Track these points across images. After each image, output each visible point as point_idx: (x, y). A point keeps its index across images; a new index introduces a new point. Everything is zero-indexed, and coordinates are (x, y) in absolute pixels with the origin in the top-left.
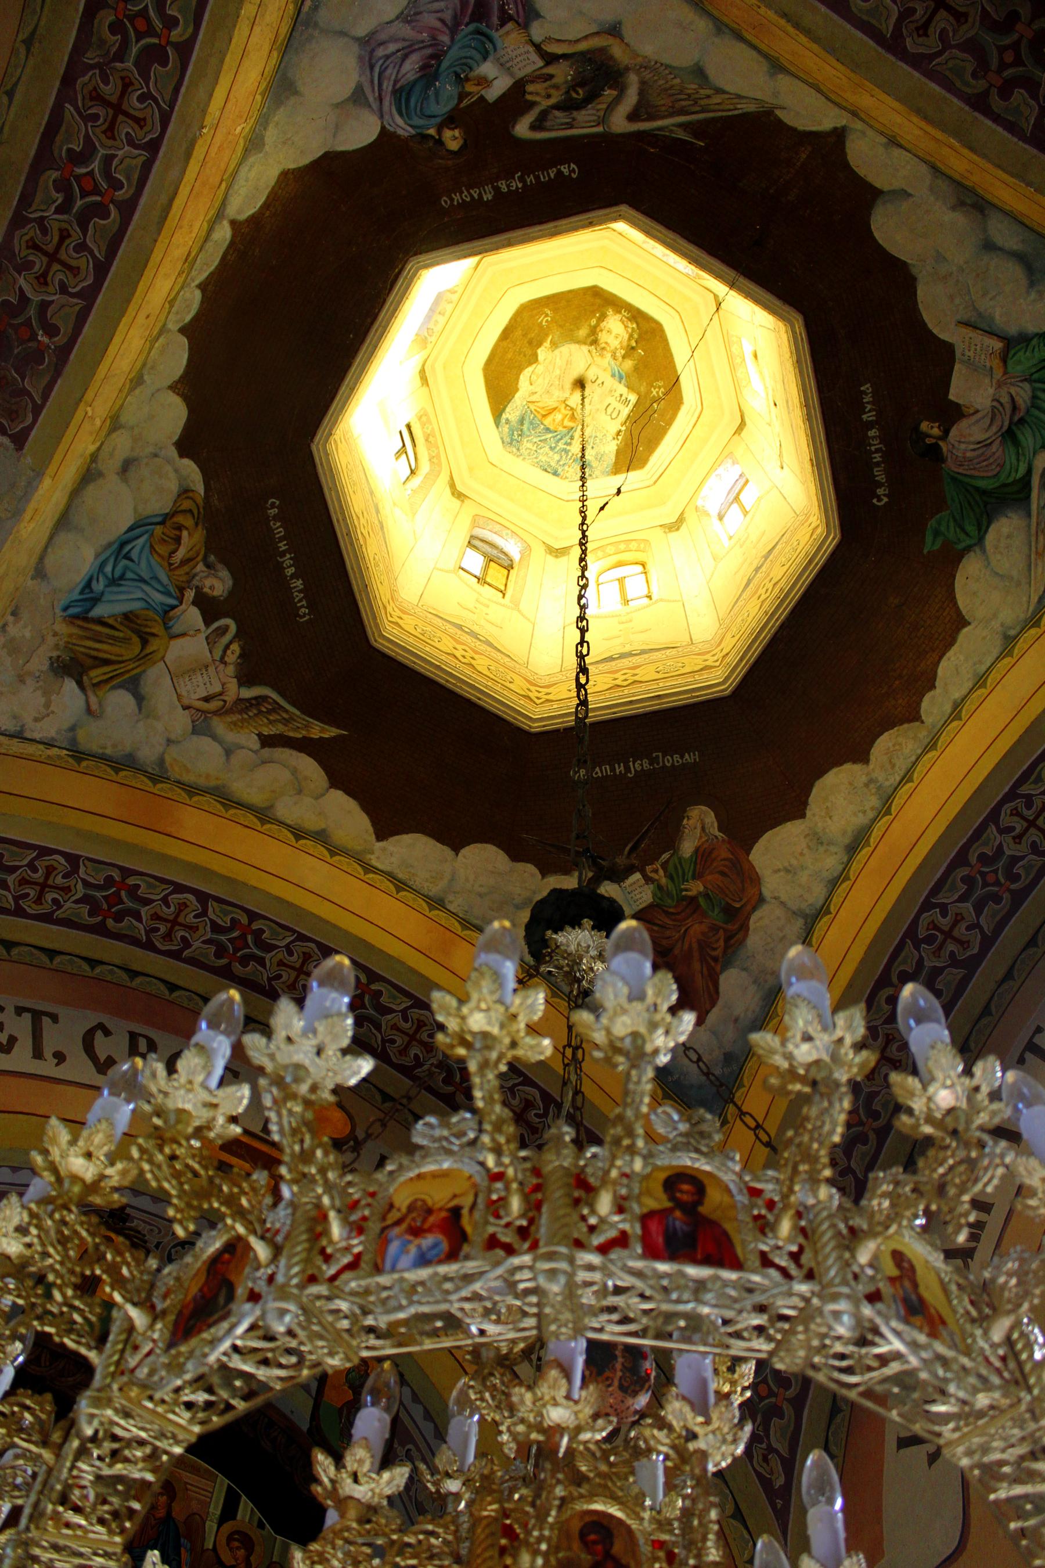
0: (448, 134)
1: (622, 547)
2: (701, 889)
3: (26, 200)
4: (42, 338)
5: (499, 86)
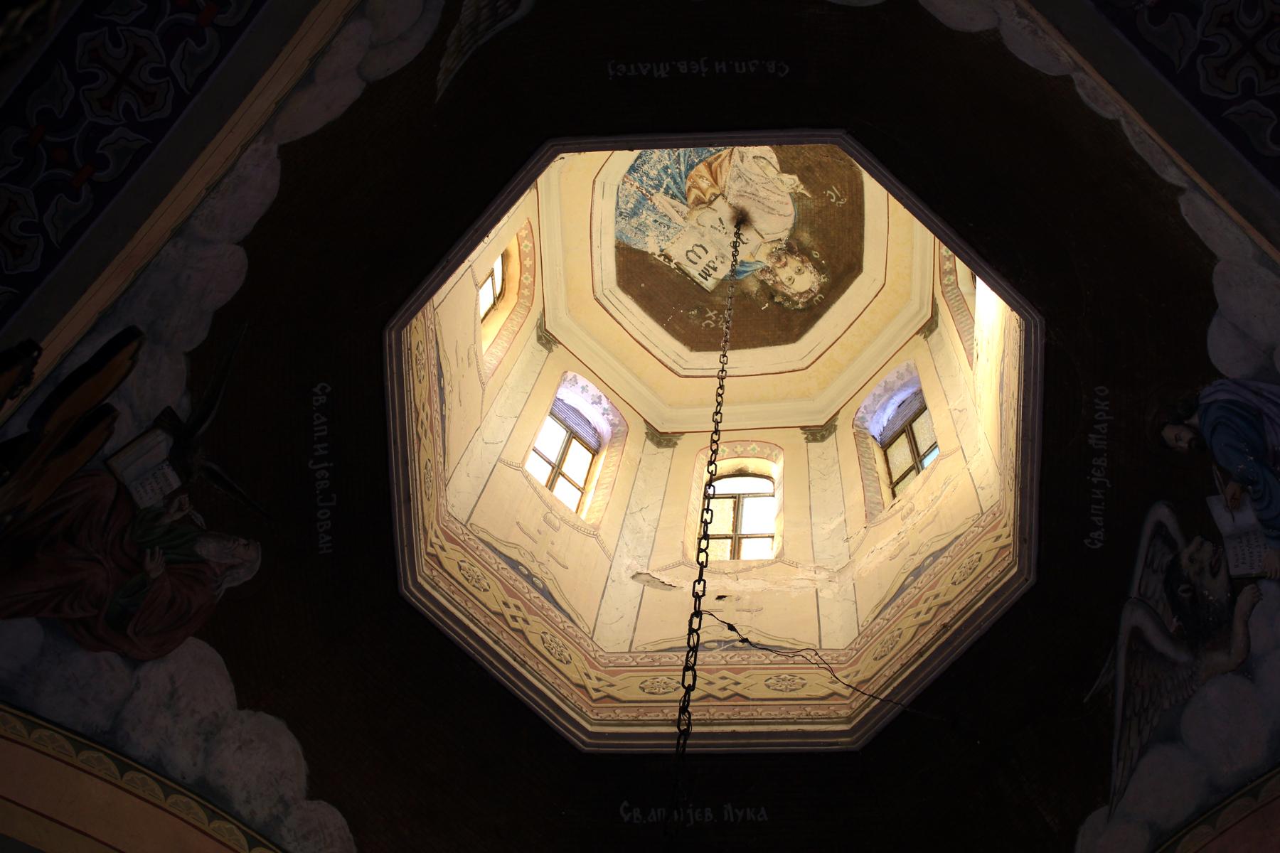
0: (1186, 435)
1: (528, 262)
2: (153, 575)
5: (1223, 519)
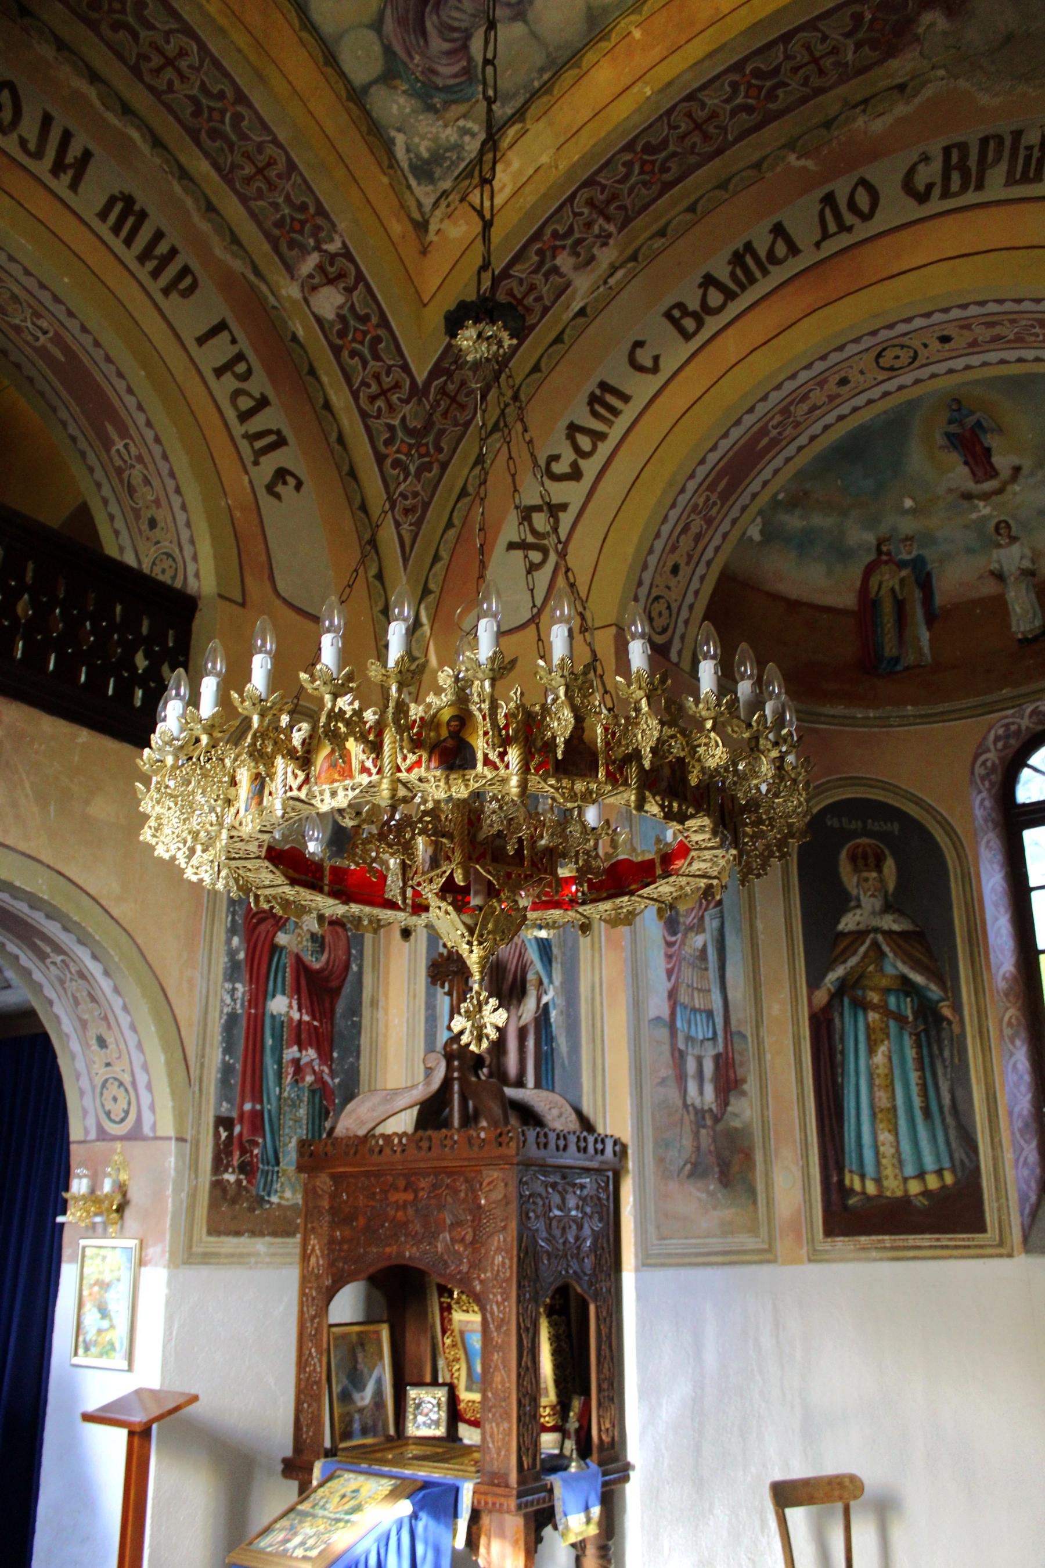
3: (804, 100)
4: (868, 16)
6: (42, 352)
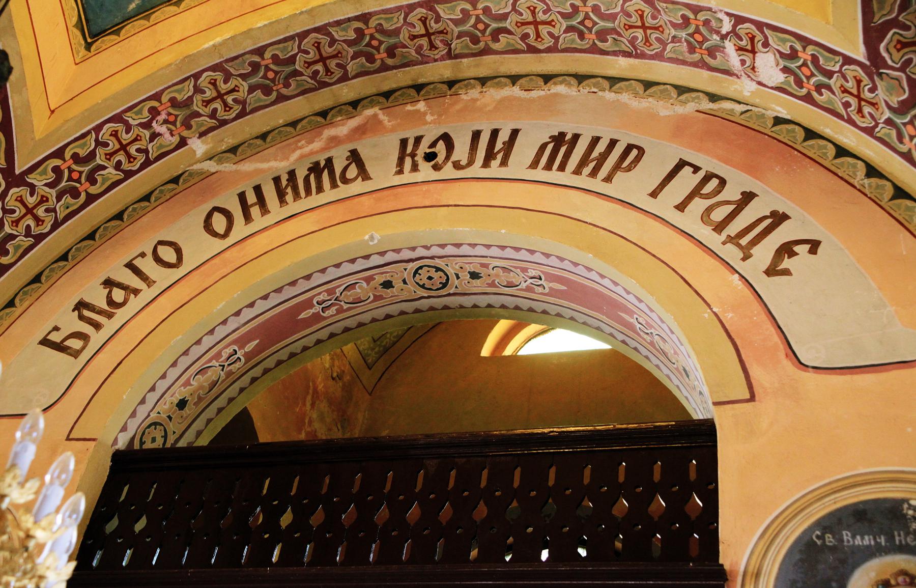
6: (553, 293)
